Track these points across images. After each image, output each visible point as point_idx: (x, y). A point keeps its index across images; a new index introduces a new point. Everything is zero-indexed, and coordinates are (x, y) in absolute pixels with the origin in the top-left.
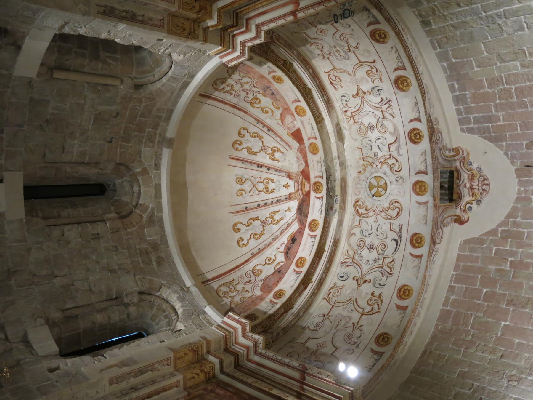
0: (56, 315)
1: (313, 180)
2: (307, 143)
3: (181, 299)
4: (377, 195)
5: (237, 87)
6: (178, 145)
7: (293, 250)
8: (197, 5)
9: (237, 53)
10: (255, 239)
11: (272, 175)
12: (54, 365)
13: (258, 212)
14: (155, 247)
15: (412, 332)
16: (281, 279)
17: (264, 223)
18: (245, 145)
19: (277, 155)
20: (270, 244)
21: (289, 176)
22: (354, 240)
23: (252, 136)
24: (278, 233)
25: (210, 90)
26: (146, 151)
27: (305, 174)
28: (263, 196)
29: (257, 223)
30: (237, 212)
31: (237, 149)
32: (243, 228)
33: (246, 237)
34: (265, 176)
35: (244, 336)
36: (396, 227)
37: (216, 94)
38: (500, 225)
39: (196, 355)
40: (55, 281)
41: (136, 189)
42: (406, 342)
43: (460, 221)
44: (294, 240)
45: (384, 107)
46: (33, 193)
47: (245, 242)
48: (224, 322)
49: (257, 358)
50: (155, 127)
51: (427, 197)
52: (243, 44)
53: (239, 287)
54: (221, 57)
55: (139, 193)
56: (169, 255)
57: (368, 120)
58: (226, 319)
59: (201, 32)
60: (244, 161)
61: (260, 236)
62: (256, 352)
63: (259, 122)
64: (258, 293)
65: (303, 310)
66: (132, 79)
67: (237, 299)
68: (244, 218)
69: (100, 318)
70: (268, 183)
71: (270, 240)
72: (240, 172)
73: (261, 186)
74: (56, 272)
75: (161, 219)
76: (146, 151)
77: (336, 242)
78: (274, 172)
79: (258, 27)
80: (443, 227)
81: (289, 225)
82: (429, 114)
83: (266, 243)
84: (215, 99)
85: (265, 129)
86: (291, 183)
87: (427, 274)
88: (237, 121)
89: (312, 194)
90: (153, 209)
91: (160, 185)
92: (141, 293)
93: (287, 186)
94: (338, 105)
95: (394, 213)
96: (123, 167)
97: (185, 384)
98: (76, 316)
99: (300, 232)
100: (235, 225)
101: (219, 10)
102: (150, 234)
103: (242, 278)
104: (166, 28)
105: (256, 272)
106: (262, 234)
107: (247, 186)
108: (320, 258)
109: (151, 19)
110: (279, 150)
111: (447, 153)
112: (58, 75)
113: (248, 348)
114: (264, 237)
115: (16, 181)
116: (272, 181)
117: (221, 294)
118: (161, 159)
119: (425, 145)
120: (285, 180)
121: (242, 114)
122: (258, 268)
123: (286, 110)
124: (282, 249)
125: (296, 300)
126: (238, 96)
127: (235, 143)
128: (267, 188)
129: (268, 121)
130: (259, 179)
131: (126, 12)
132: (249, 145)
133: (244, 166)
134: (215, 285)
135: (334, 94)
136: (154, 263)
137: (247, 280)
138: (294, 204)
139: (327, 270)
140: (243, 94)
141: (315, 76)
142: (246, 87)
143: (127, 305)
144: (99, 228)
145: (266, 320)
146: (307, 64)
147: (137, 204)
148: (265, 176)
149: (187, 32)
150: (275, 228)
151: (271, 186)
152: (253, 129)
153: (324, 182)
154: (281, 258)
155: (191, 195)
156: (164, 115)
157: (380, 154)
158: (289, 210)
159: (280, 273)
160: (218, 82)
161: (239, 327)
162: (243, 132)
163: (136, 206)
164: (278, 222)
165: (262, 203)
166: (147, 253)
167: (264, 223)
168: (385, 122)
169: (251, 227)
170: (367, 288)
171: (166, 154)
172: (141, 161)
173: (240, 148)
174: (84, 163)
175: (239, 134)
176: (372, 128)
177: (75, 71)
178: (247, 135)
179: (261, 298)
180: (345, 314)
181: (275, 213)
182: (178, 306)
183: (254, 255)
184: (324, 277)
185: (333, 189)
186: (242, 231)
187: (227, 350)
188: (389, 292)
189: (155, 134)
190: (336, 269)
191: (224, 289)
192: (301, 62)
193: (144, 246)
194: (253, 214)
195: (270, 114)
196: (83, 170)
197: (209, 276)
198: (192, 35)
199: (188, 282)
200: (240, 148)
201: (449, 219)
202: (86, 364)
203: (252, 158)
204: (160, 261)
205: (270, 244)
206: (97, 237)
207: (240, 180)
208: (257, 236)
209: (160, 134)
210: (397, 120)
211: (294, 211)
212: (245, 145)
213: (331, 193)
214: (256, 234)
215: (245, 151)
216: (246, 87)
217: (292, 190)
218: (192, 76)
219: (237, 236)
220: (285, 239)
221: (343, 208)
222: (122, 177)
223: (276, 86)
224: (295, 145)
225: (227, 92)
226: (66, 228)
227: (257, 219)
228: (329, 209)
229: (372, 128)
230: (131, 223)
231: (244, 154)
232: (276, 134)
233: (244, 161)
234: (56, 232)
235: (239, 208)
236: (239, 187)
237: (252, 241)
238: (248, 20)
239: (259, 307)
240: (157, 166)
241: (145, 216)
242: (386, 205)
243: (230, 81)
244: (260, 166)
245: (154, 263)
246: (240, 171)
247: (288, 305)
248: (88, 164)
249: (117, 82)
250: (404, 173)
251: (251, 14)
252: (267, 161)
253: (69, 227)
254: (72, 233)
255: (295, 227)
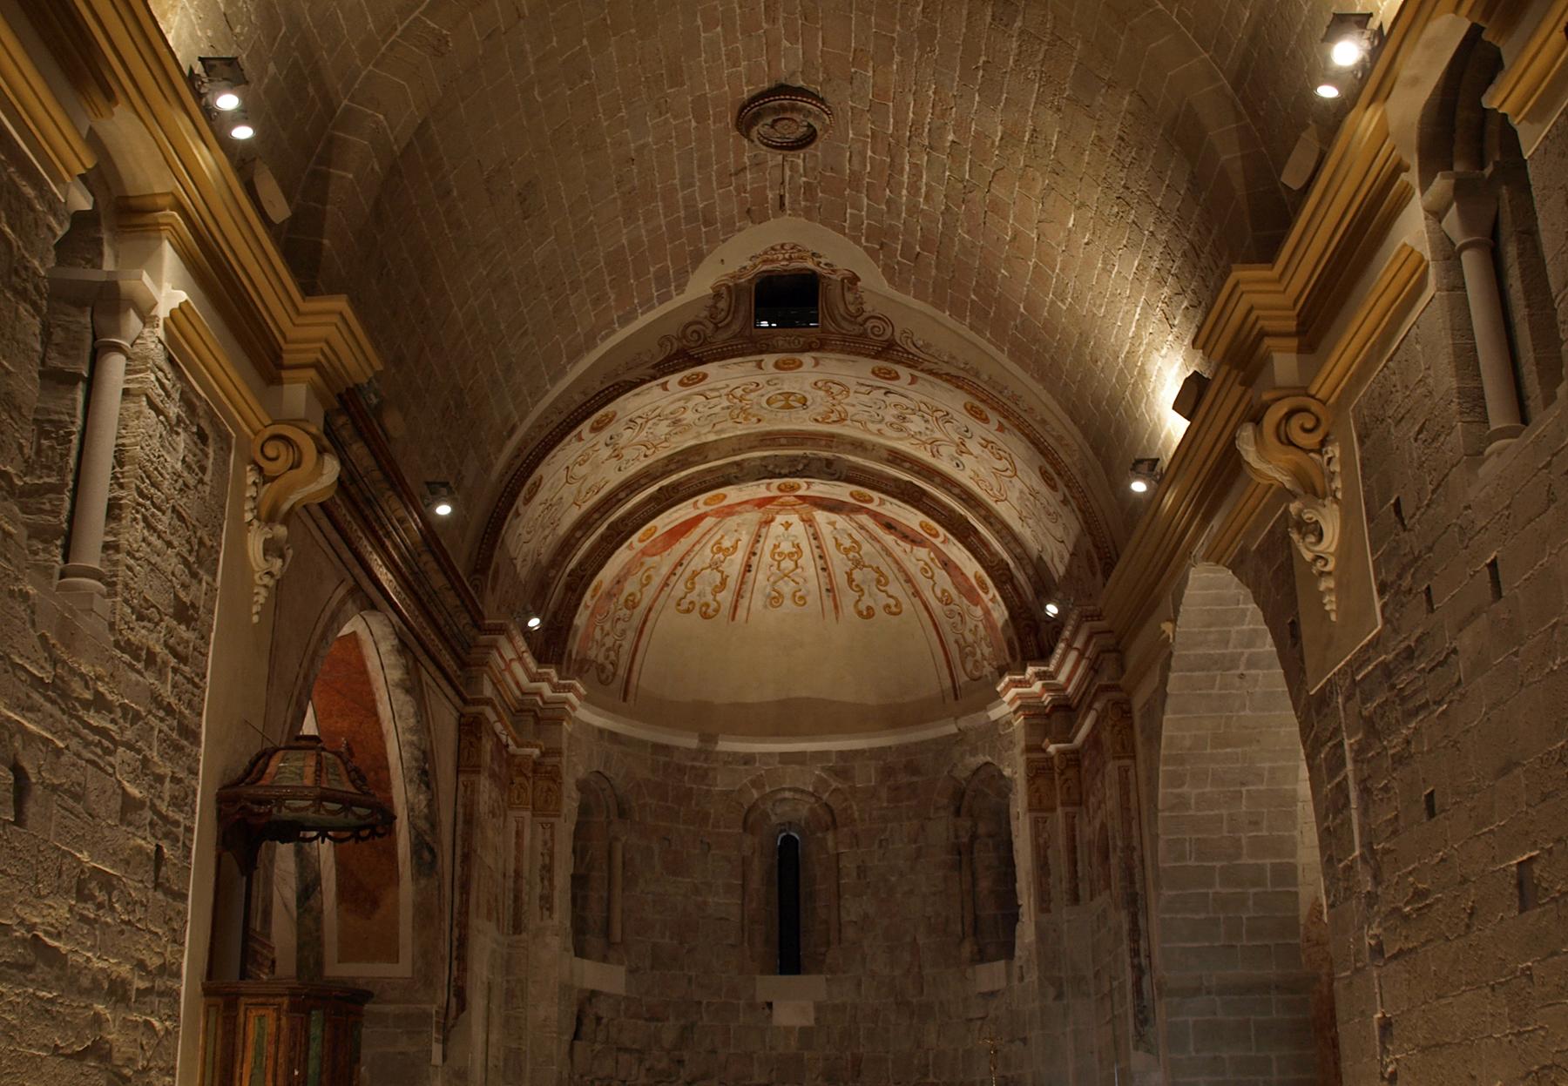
0: (967, 949)
1: (774, 492)
2: (703, 509)
3: (974, 751)
4: (804, 402)
5: (609, 642)
6: (707, 718)
7: (908, 533)
8: (517, 780)
9: (571, 696)
10: (886, 584)
11: (767, 546)
12: (1016, 971)
13: (838, 571)
14: (887, 772)
15: (1043, 422)
16: (957, 567)
17: (858, 564)
18: (709, 598)
19: (727, 543)
20: (897, 562)
21: (768, 522)
22: (888, 432)
23: (693, 589)
24: (878, 546)
25: (617, 685)
26: (722, 783)
27: (761, 503)
28: (807, 560)
29: (857, 574)
30: (836, 607)
31: (717, 611)
32: (867, 601)
33: (883, 599)
34: (767, 558)
35: (1028, 684)
36: (863, 389)
37: (622, 672)
38: (857, 241)
39: (1039, 770)
40: (921, 941)
41: (787, 794)
42: (1059, 439)
43: (854, 279)
44: (889, 526)
45: (639, 421)
46: (790, 960)
47: (892, 602)
48: (1012, 701)
49: (1062, 678)
50: (681, 769)
51: (807, 359)
52: (555, 688)
53: (970, 638)
54: (574, 708)
55: (796, 790)
56: (903, 749)
57: (663, 428)
58: (1007, 698)
59: (549, 760)
60: (739, 595)
61: (882, 574)
62: (1052, 676)
63: (666, 584)
64: (979, 612)
65: (1013, 545)
66: (610, 823)
67: (987, 651)
68: (848, 599)
69: (985, 884)
70: (780, 554)
71: (889, 560)
72: (758, 601)
73: (788, 564)
74: (908, 939)
75: (841, 754)
76: (722, 783)
77: (896, 458)
78: (759, 545)
79: (533, 680)
80: (866, 315)
81: (862, 527)
82: (654, 367)
83: (894, 566)
84: (630, 670)
85: (680, 570)
86: (780, 519)
87: (946, 369)
88: (667, 622)
89: (799, 493)
90: (823, 769)
91: (781, 754)
92: (958, 813)
93: (787, 525)
94: (632, 470)
95: (836, 389)
96: (750, 820)
97: (1074, 804)
98: (976, 918)
99: (875, 516)
100: (860, 613)
101: (518, 745)
102: (867, 776)
103: (954, 626)
104: (552, 820)
105: (947, 601)
106: (877, 570)
107: (787, 588)
108: (924, 492)
109: (545, 843)
110: (718, 542)
111: (722, 304)
112: (617, 935)
113: (1046, 688)
114: (884, 569)
115: (770, 985)
116: (776, 547)
117: (977, 674)
118: (735, 754)
119: (711, 369)
120: (776, 528)
121: (652, 615)
122: (939, 594)
123: (644, 552)
124: (908, 547)
125: (994, 554)
126: (624, 632)
127: (705, 616)
128: (791, 555)
129: (665, 570)
130: (774, 569)
131: (542, 879)
132: (708, 590)
133: (748, 595)
134: (963, 679)
135: (613, 478)
136: (915, 779)
137: (958, 618)
138: (821, 516)
139: (947, 483)
140: (620, 625)
141: (585, 524)
142: (607, 627)
143: (974, 837)
144: (849, 865)
145: (1016, 628)
146: (567, 545)
147: (812, 795)
148: (767, 558)
149: (552, 785)
150: (866, 547)
151: (786, 547)
152: (680, 589)
153: (777, 482)
154: (922, 553)
155: (802, 692)
156: (662, 759)
157: (726, 404)
158: (833, 524)
159: (947, 564)
160: (603, 677)
161: (1013, 692)
162: (685, 605)
163: (818, 799)
164: (855, 541)
165: (820, 563)
166: (897, 788)
167: (858, 564)
168: (667, 411)
169: (865, 588)
170: (973, 446)
171: (725, 745)
172: (740, 790)
173: (713, 605)
174: (743, 886)
175: (688, 611)
176: (676, 422)
177: (609, 909)
178: (690, 597)
179: (987, 612)
180: (1017, 494)
181: (838, 545)
182: (982, 759)
183: (917, 593)
184: (957, 491)
185: (793, 460)
186: (871, 604)
187: (1048, 716)
188: (976, 427)
189: (693, 767)
190: (945, 466)
191: (969, 666)
192: (566, 556)
193: (884, 793)
194: (841, 580)
195: (652, 572)
196: (756, 881)
197: (948, 683)
198: (554, 776)
199: (951, 729)
200: (713, 605)
201: (849, 297)
202: (1026, 932)
203: (732, 583)
204: (912, 768)
205: (897, 562)
206: (862, 870)
207: (775, 599)
208: (881, 580)
209: (694, 759)
210: (664, 402)
211: (833, 517)
212: (709, 598)
213: (800, 467)
214: (879, 582)
215: (719, 597)
216: (607, 627)
217: (794, 518)
218: (601, 731)
219: (880, 613)
220: (889, 539)
221: (831, 440)
222: (768, 816)
223: (605, 586)
224: (709, 522)
225: (617, 654)
226: (845, 918)
227: (849, 575)
228: (830, 470)
229: (676, 422)
230: (845, 809)
231: (726, 597)
232: (688, 553)
233: (739, 595)
234: (850, 933)
235: (829, 604)
236: (788, 602)
237: (891, 589)
238: (523, 693)
239: (1000, 624)
240: (748, 759)
241: (834, 785)
242: (822, 393)
243: (601, 659)
244: (748, 568)
245: (915, 779)
246: (756, 601)
247: (999, 574)
248: (744, 877)
249: (619, 847)
250: (761, 379)
251: (518, 693)
252: (739, 558)
253: (843, 914)
254: (852, 909)
255: (863, 518)
